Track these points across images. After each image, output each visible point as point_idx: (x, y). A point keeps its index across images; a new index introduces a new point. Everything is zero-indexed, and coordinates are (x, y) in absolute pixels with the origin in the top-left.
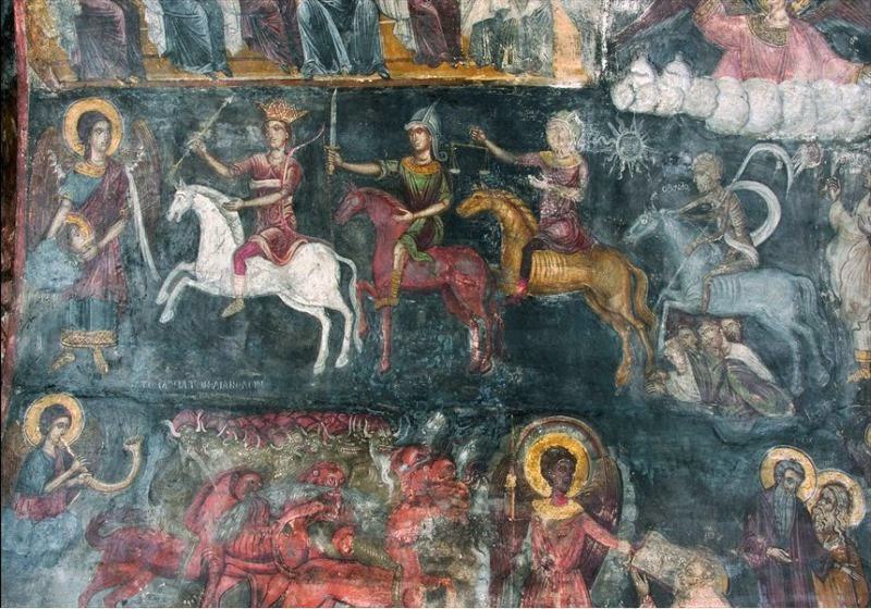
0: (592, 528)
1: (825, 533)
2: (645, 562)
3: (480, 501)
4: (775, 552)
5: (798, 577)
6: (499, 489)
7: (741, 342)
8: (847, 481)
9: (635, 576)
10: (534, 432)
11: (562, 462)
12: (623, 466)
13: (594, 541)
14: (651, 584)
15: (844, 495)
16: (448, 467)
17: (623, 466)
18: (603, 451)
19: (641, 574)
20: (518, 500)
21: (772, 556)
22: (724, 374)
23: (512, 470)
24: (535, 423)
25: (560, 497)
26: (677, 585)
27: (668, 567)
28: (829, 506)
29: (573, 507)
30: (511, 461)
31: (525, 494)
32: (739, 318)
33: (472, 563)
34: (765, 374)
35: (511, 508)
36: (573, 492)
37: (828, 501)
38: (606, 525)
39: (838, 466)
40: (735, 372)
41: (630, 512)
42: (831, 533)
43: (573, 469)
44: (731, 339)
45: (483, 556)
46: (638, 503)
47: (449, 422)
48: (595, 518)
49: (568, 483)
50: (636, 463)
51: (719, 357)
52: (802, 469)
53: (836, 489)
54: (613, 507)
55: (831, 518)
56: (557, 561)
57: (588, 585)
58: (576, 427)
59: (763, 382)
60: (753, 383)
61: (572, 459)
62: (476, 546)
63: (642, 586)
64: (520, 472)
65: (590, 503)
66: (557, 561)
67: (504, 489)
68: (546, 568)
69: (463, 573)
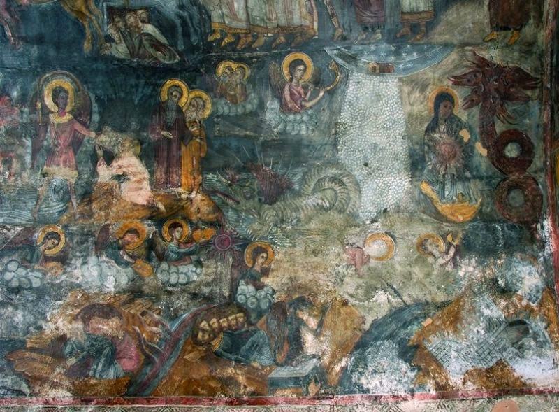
0: (78, 126)
1: (190, 123)
2: (102, 142)
3: (25, 116)
4: (165, 133)
5: (174, 146)
6: (33, 109)
7: (149, 23)
8: (204, 96)
9: (97, 148)
10: (47, 80)
11: (62, 94)
12: (91, 95)
13: (79, 132)
14: (104, 152)
15: (202, 103)
16: (8, 100)
17: (91, 95)
18: (81, 88)
19: (100, 147)
20: (42, 115)
21: (163, 135)
22: (141, 42)
23: (38, 100)
24: (47, 75)
25: (62, 112)
26: (117, 151)
27: (112, 144)
28: (194, 109)
29: (68, 117)
30: (39, 95)
31: (46, 112)
32: (146, 9)
33: (23, 146)
34: (163, 40)
35: (39, 118)
36: (68, 109)
37: (194, 106)
38: (84, 124)
39: (200, 88)
40: (146, 40)
41: (96, 117)
42: (193, 122)
43: (67, 98)
44: (143, 22)
45: (28, 142)
46: (100, 113)
47: (5, 77)
48: (80, 122)
49: (66, 104)
50: (98, 92)
51: (138, 32)
52: (182, 91)
53: (197, 100)
54: (88, 115)
55: (194, 115)
56: (62, 143)
57: (75, 154)
58: (68, 76)
59: (164, 46)
60: (157, 45)
61: (66, 92)
62: (25, 137)
63: (100, 153)
64: (42, 100)
65: (77, 114)
66: (62, 143)
67: (36, 110)
68: (56, 146)
69: (20, 151)
